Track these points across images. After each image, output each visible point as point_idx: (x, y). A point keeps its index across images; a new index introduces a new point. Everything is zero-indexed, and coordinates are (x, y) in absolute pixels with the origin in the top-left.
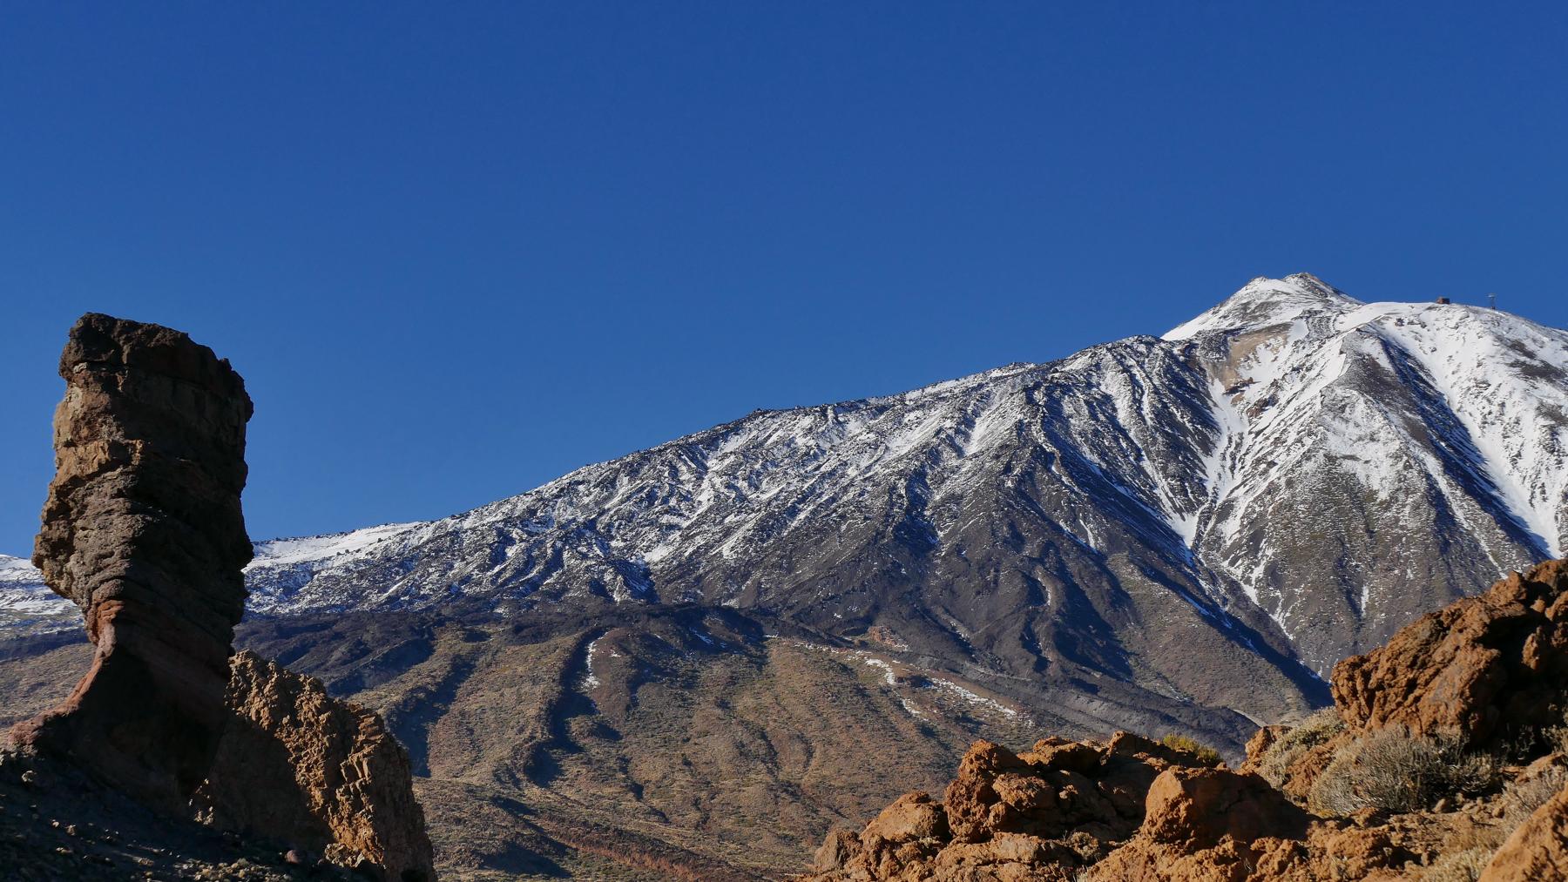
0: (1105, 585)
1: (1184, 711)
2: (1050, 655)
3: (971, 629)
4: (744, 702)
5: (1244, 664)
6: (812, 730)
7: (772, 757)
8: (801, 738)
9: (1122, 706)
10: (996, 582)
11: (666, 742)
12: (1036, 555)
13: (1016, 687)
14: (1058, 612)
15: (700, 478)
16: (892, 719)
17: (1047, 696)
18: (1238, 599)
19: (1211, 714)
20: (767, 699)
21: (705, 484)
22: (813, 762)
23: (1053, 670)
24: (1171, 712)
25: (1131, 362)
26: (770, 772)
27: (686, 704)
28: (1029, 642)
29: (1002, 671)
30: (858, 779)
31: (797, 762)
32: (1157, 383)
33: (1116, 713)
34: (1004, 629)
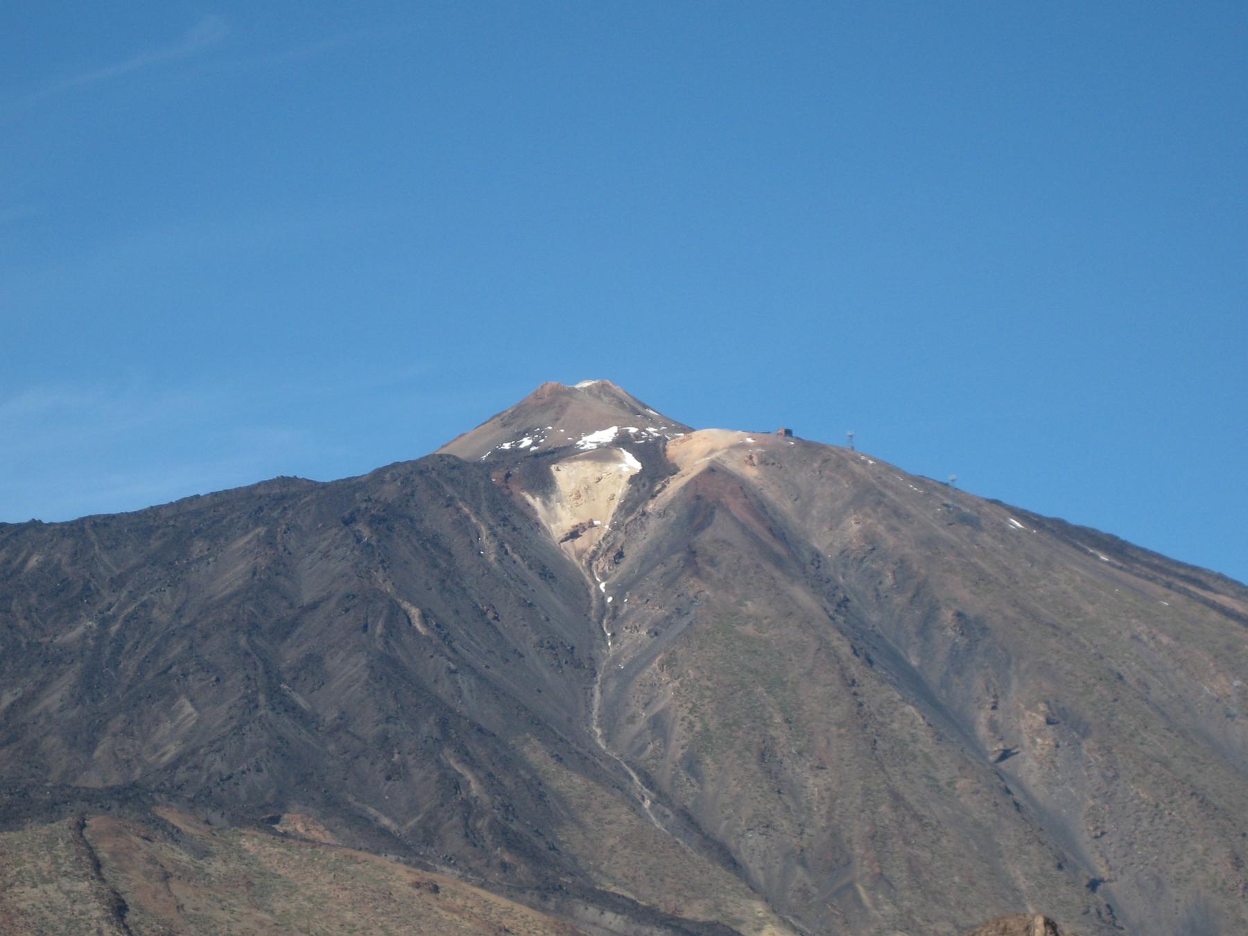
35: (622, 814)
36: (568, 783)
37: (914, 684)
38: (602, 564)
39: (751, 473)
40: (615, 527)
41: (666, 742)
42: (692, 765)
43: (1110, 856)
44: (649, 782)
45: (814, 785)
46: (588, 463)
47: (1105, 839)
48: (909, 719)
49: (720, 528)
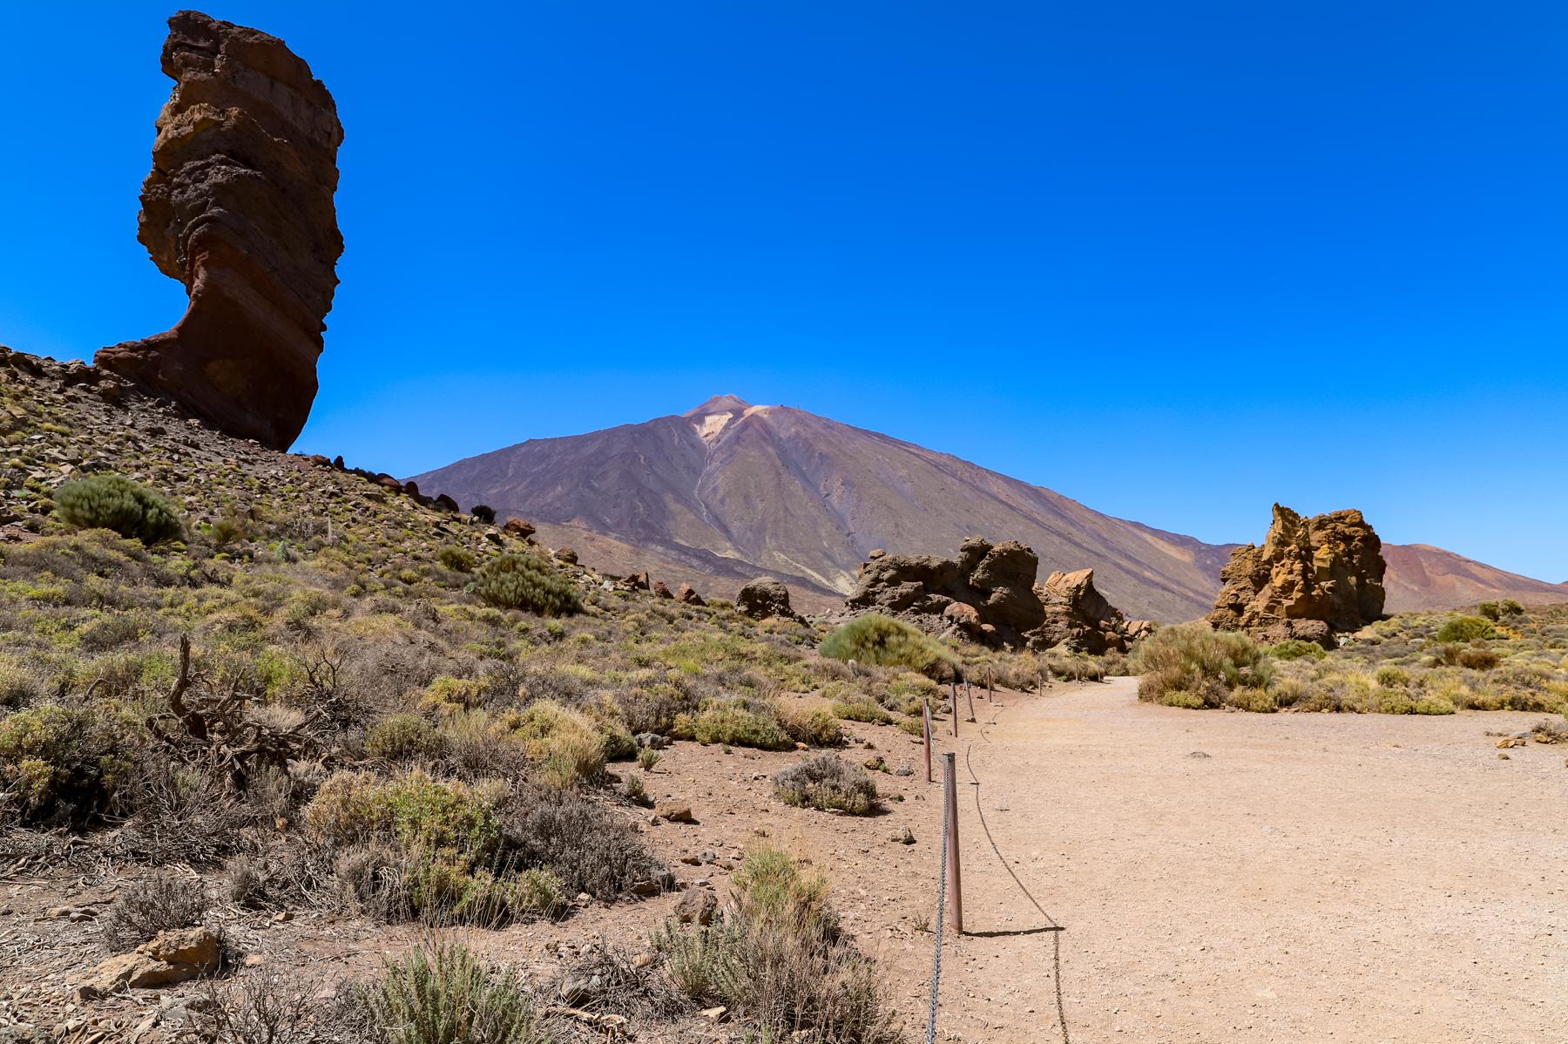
35: (691, 517)
36: (674, 507)
37: (803, 475)
42: (722, 501)
44: (707, 506)
45: (760, 506)
48: (796, 485)
49: (750, 431)
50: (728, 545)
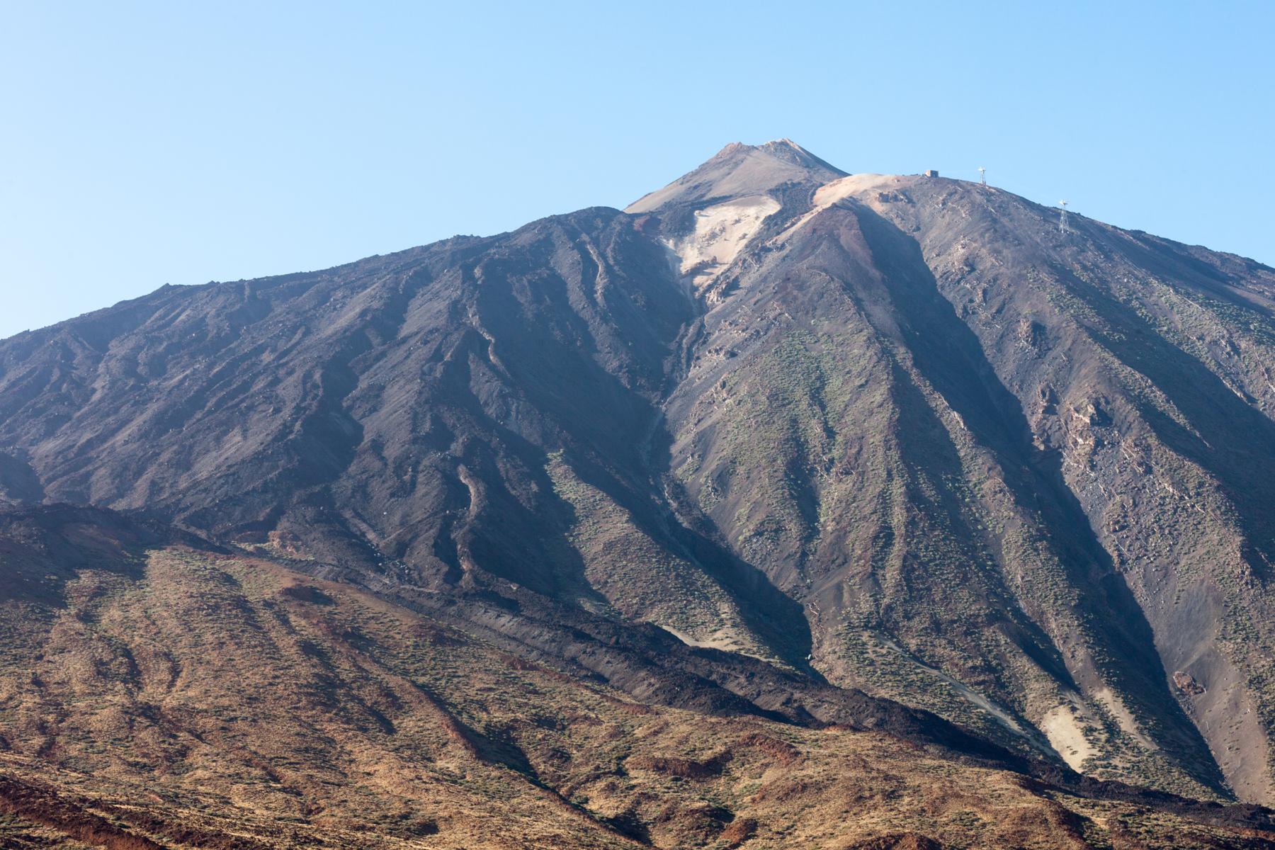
0: (534, 487)
1: (604, 627)
2: (465, 565)
3: (382, 534)
4: (111, 615)
5: (678, 576)
6: (182, 649)
7: (134, 676)
8: (167, 656)
9: (531, 620)
10: (413, 483)
11: (17, 659)
12: (459, 454)
13: (420, 600)
14: (478, 517)
15: (98, 360)
16: (273, 634)
17: (452, 610)
18: (680, 503)
19: (633, 631)
20: (135, 613)
21: (101, 368)
22: (179, 683)
23: (466, 581)
24: (588, 629)
25: (585, 237)
26: (130, 693)
27: (49, 619)
28: (443, 548)
29: (410, 582)
30: (225, 701)
31: (161, 682)
32: (611, 262)
33: (525, 629)
34: (416, 536)
38: (713, 296)
39: (878, 208)
40: (736, 264)
41: (702, 457)
43: (1124, 550)
46: (732, 208)
47: (1124, 533)
50: (725, 609)
